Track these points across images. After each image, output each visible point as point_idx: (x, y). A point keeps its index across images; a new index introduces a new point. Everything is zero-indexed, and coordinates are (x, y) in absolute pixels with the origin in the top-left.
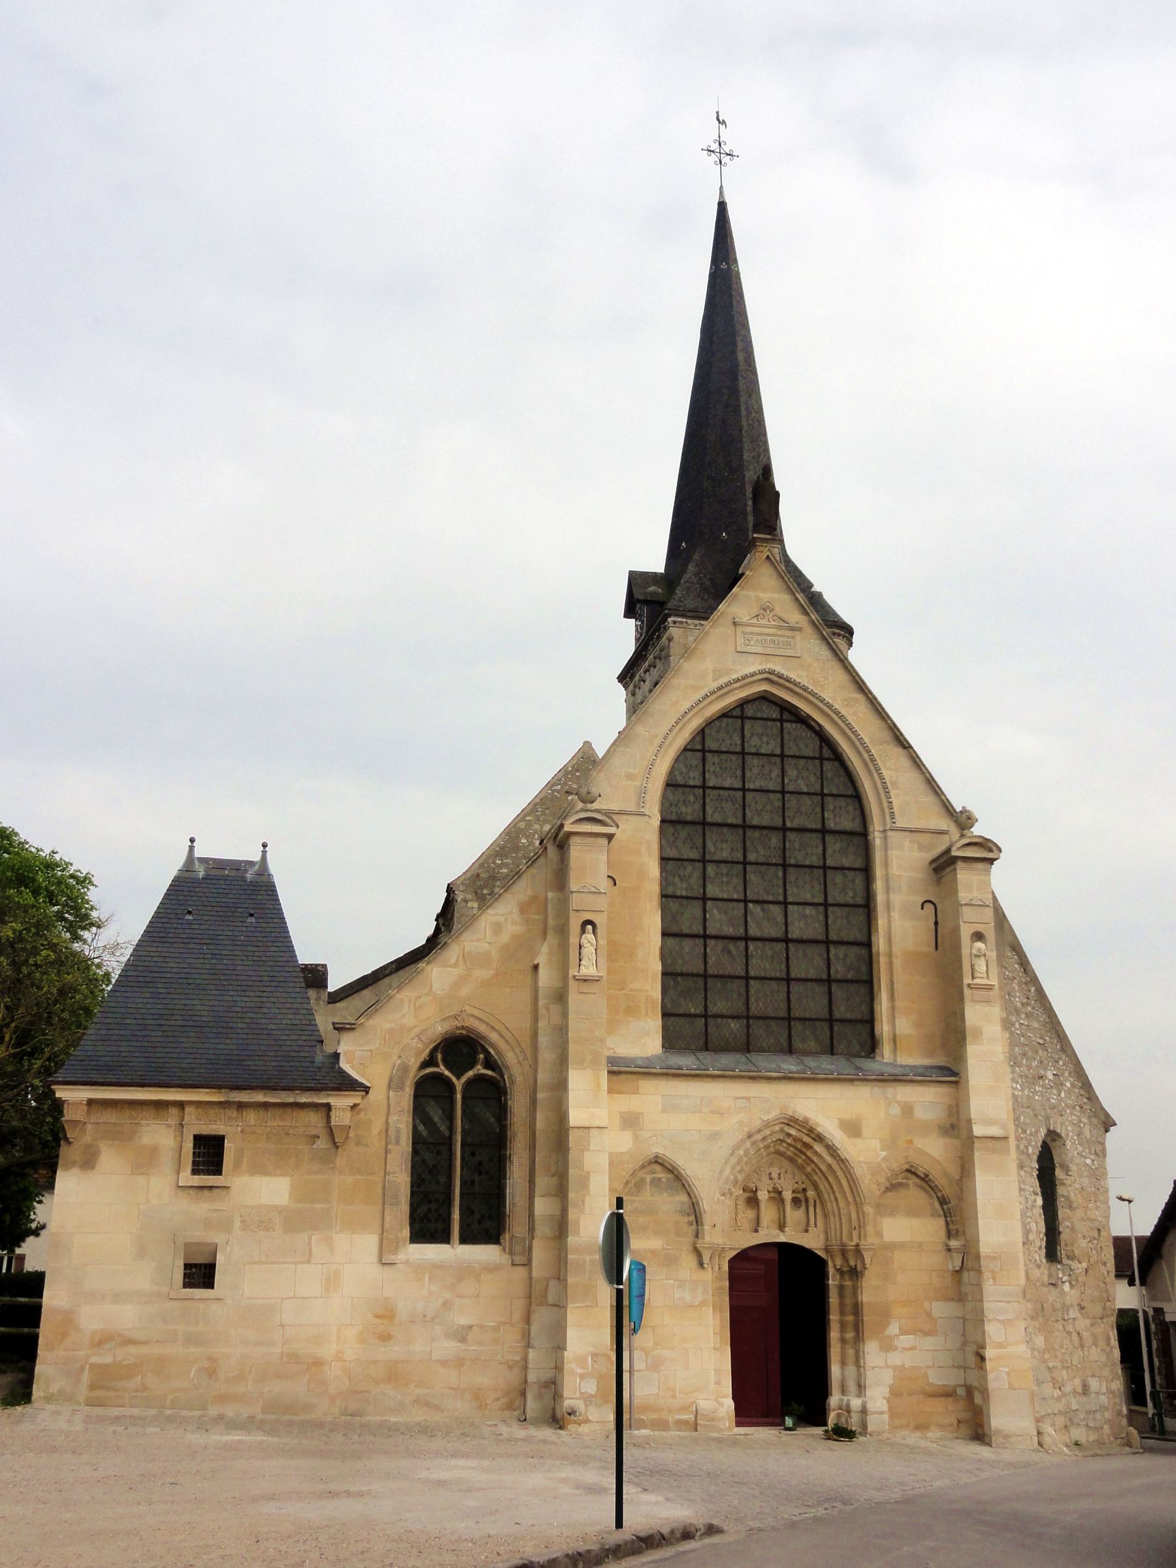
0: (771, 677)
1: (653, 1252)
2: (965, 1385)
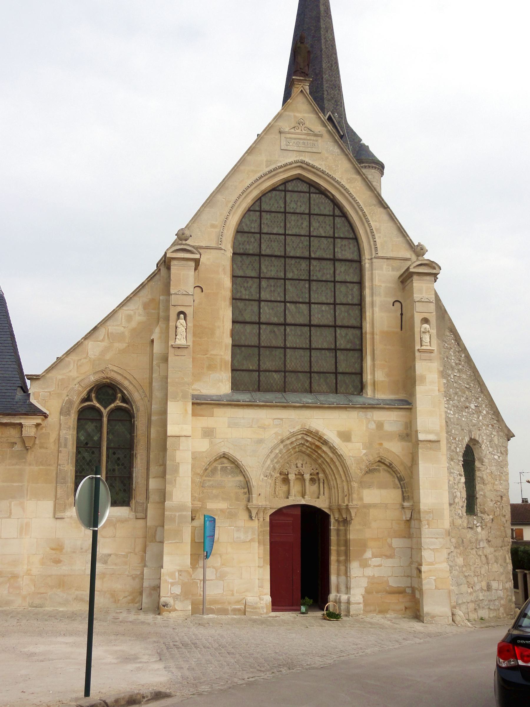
0: (303, 165)
1: (222, 511)
2: (411, 587)
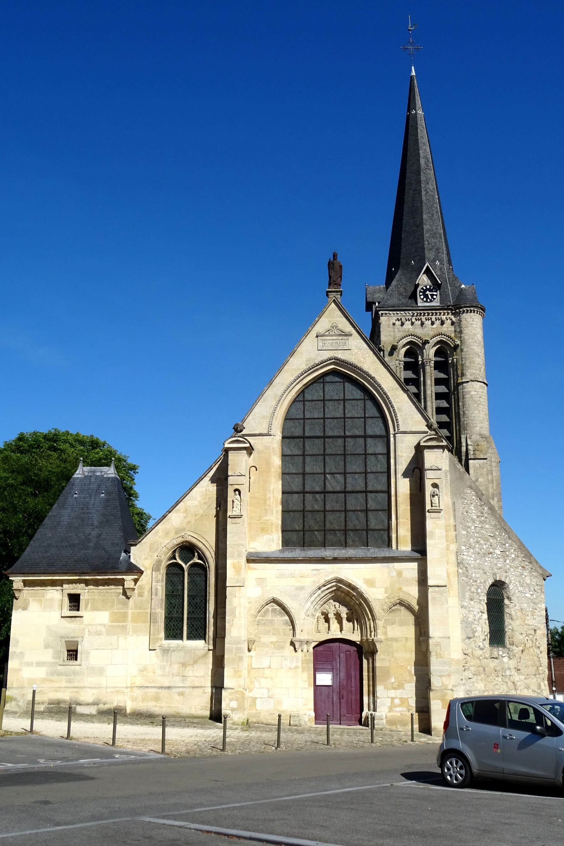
0: (338, 361)
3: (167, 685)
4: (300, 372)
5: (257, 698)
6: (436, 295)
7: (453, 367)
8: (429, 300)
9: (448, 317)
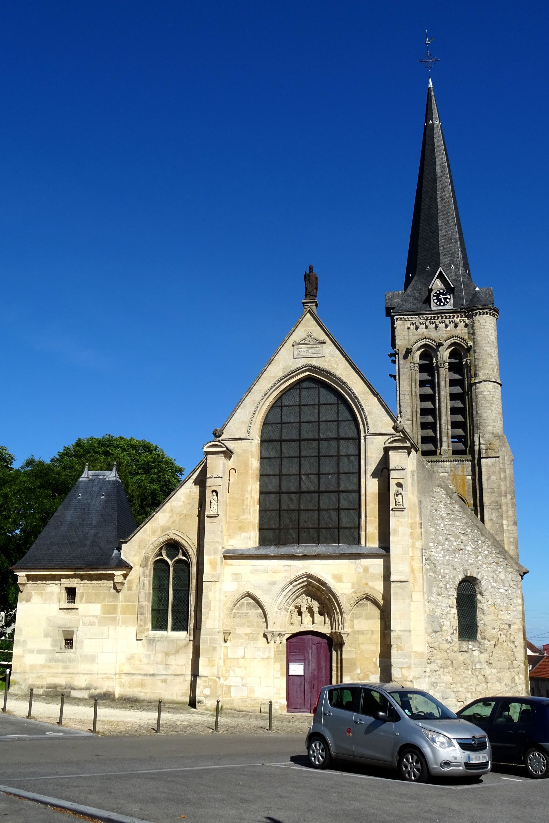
3: (152, 672)
4: (277, 379)
5: (231, 686)
6: (450, 299)
7: (467, 368)
8: (442, 304)
9: (461, 320)
